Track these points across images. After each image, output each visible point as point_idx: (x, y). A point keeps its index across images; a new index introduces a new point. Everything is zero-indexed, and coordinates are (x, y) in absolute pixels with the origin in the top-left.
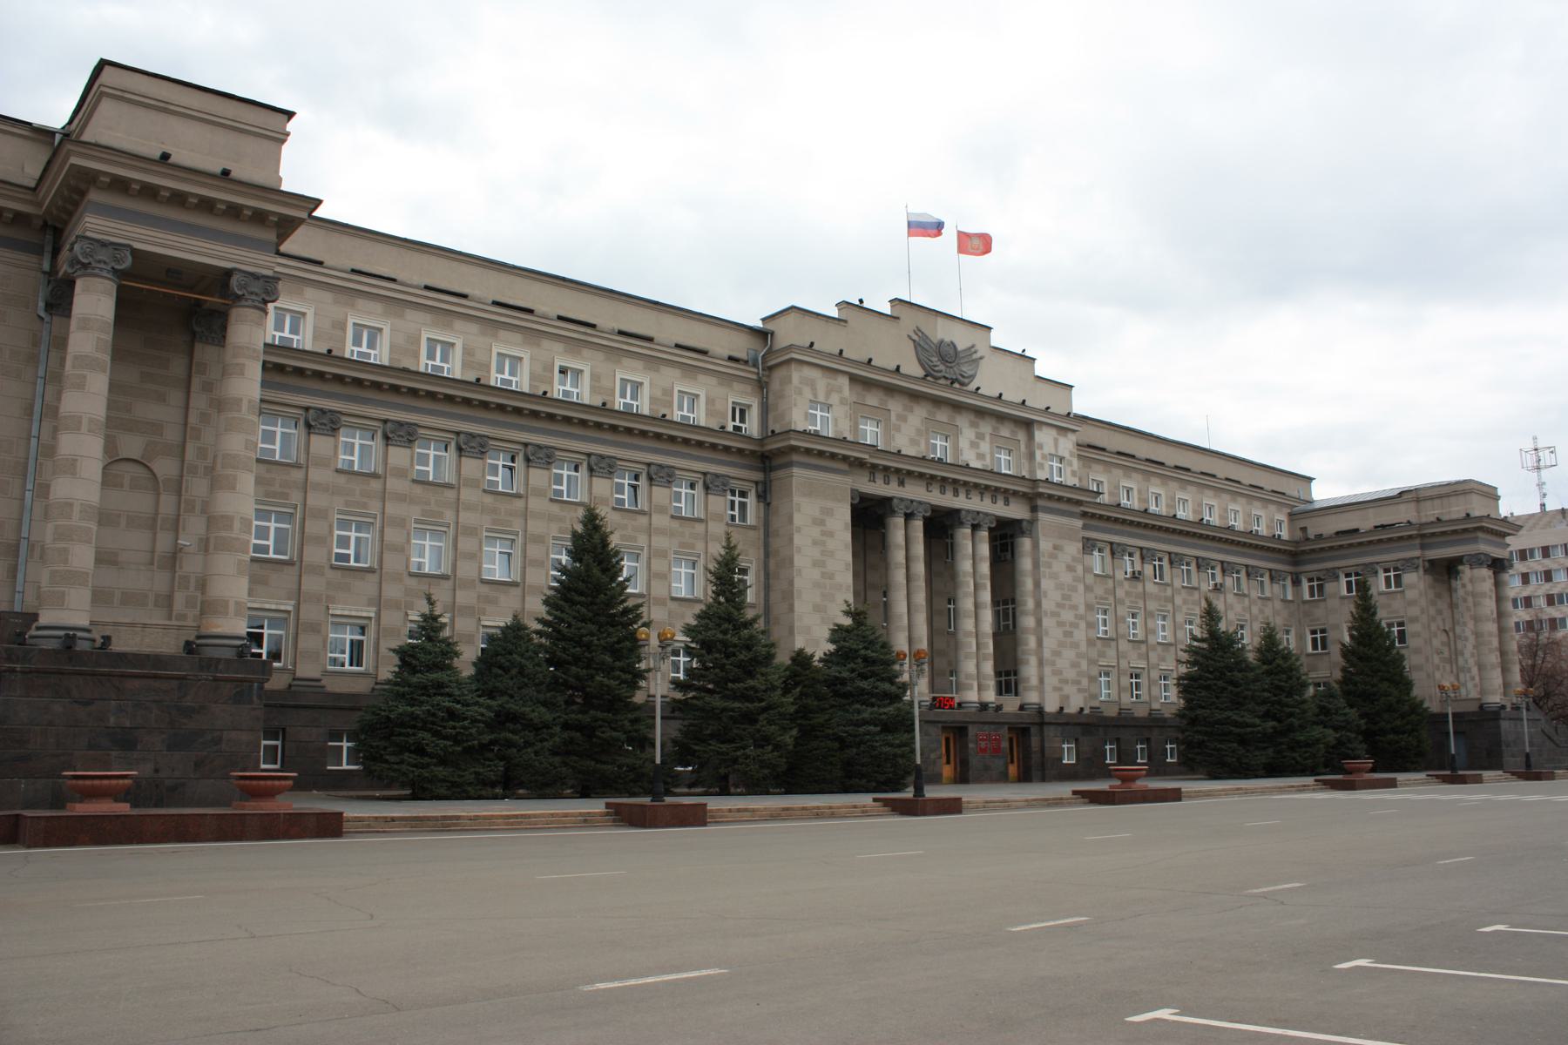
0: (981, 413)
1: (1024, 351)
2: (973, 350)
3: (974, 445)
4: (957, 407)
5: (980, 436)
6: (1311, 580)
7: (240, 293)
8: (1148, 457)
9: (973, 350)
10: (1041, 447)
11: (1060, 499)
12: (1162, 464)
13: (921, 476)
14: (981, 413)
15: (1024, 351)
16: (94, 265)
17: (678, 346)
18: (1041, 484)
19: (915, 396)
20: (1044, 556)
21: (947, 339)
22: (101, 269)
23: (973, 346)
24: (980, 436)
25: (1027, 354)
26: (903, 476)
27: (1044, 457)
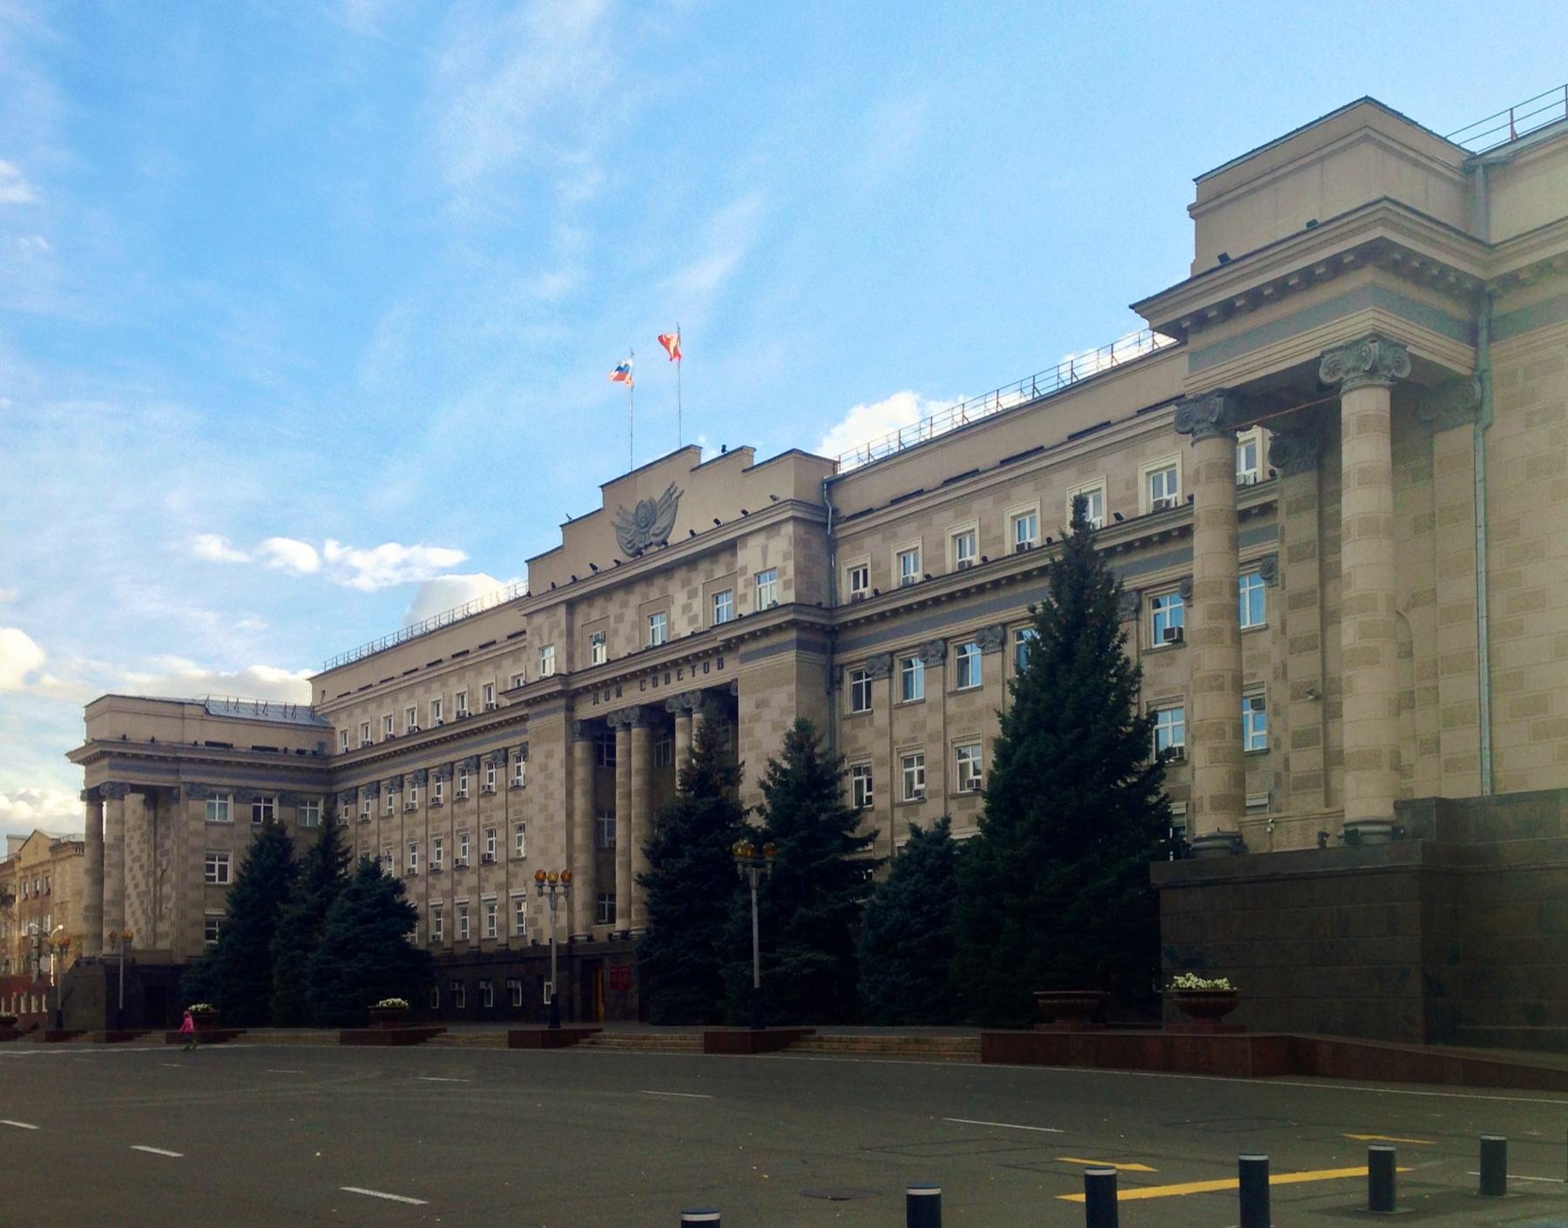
0: (691, 562)
1: (724, 447)
2: (672, 491)
3: (686, 608)
4: (667, 571)
5: (692, 595)
6: (858, 676)
7: (1335, 379)
8: (1003, 457)
9: (672, 491)
10: (744, 570)
11: (766, 632)
12: (1040, 449)
13: (634, 675)
14: (691, 562)
15: (723, 450)
16: (1346, 378)
17: (510, 637)
18: (715, 632)
19: (627, 585)
20: (744, 723)
21: (646, 499)
22: (1352, 380)
23: (674, 483)
24: (692, 595)
25: (729, 449)
26: (617, 684)
27: (748, 584)
